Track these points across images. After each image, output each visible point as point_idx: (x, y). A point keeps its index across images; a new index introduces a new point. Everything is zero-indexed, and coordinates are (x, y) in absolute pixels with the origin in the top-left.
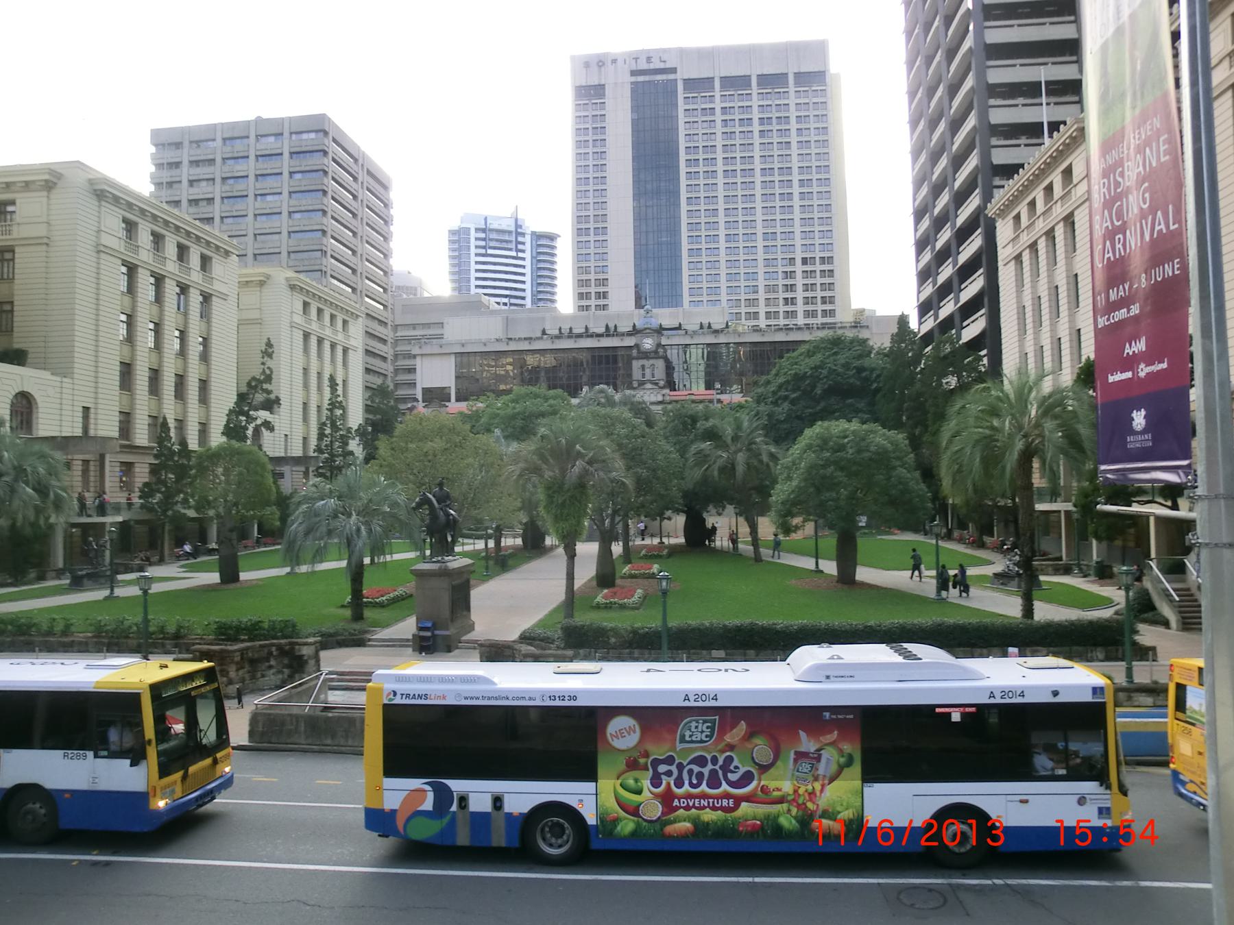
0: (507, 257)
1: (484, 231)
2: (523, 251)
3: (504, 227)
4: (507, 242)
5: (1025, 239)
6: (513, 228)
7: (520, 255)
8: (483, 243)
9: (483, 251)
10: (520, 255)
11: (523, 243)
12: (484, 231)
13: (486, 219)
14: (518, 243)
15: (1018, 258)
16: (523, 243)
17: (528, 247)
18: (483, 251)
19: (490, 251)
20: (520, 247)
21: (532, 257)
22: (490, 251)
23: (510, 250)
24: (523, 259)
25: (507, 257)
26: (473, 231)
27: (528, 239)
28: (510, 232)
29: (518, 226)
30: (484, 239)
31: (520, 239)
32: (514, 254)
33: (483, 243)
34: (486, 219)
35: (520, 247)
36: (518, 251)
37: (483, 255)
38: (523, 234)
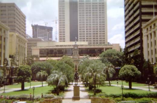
5: (149, 32)
15: (147, 36)
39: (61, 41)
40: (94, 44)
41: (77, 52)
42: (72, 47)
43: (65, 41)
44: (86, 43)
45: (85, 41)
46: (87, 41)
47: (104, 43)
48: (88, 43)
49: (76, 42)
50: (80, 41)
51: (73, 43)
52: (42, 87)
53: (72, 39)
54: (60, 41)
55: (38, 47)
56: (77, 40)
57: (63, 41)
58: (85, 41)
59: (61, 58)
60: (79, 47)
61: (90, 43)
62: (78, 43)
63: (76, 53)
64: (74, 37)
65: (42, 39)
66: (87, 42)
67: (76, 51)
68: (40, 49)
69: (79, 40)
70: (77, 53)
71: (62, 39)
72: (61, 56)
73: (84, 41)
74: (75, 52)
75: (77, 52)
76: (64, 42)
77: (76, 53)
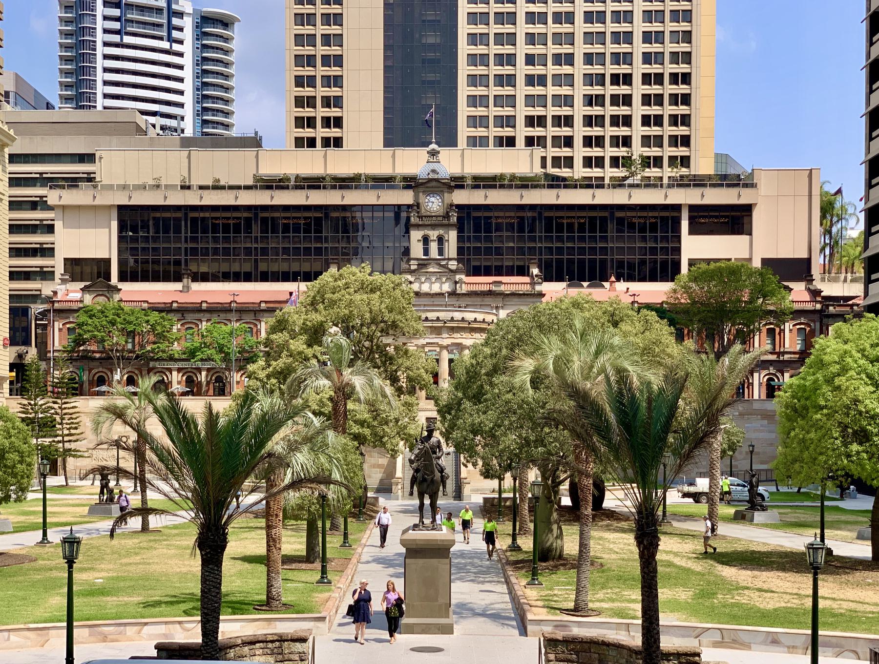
2: (181, 42)
4: (154, 25)
7: (176, 47)
8: (116, 25)
9: (116, 38)
10: (176, 47)
11: (181, 29)
14: (171, 27)
16: (181, 29)
17: (188, 35)
18: (116, 38)
19: (128, 39)
20: (175, 34)
22: (128, 39)
23: (161, 38)
24: (181, 55)
27: (187, 23)
28: (159, 10)
30: (118, 19)
31: (175, 21)
32: (165, 45)
33: (116, 25)
35: (175, 34)
36: (171, 40)
37: (117, 45)
38: (180, 15)
39: (312, 143)
40: (596, 172)
41: (440, 240)
42: (406, 197)
43: (338, 142)
44: (520, 162)
45: (520, 142)
46: (530, 141)
47: (685, 161)
48: (544, 159)
49: (434, 153)
50: (473, 142)
51: (412, 161)
52: (144, 537)
53: (400, 131)
54: (299, 142)
55: (110, 187)
56: (450, 140)
57: (326, 142)
58: (520, 142)
59: (301, 287)
60: (461, 197)
61: (557, 162)
62: (450, 162)
63: (434, 246)
64: (418, 105)
65: (141, 120)
66: (539, 152)
67: (434, 234)
68: (122, 209)
69: (464, 131)
70: (441, 251)
71: (317, 123)
72: (308, 277)
73: (511, 142)
74: (426, 240)
75: (440, 240)
76: (332, 151)
77: (434, 246)
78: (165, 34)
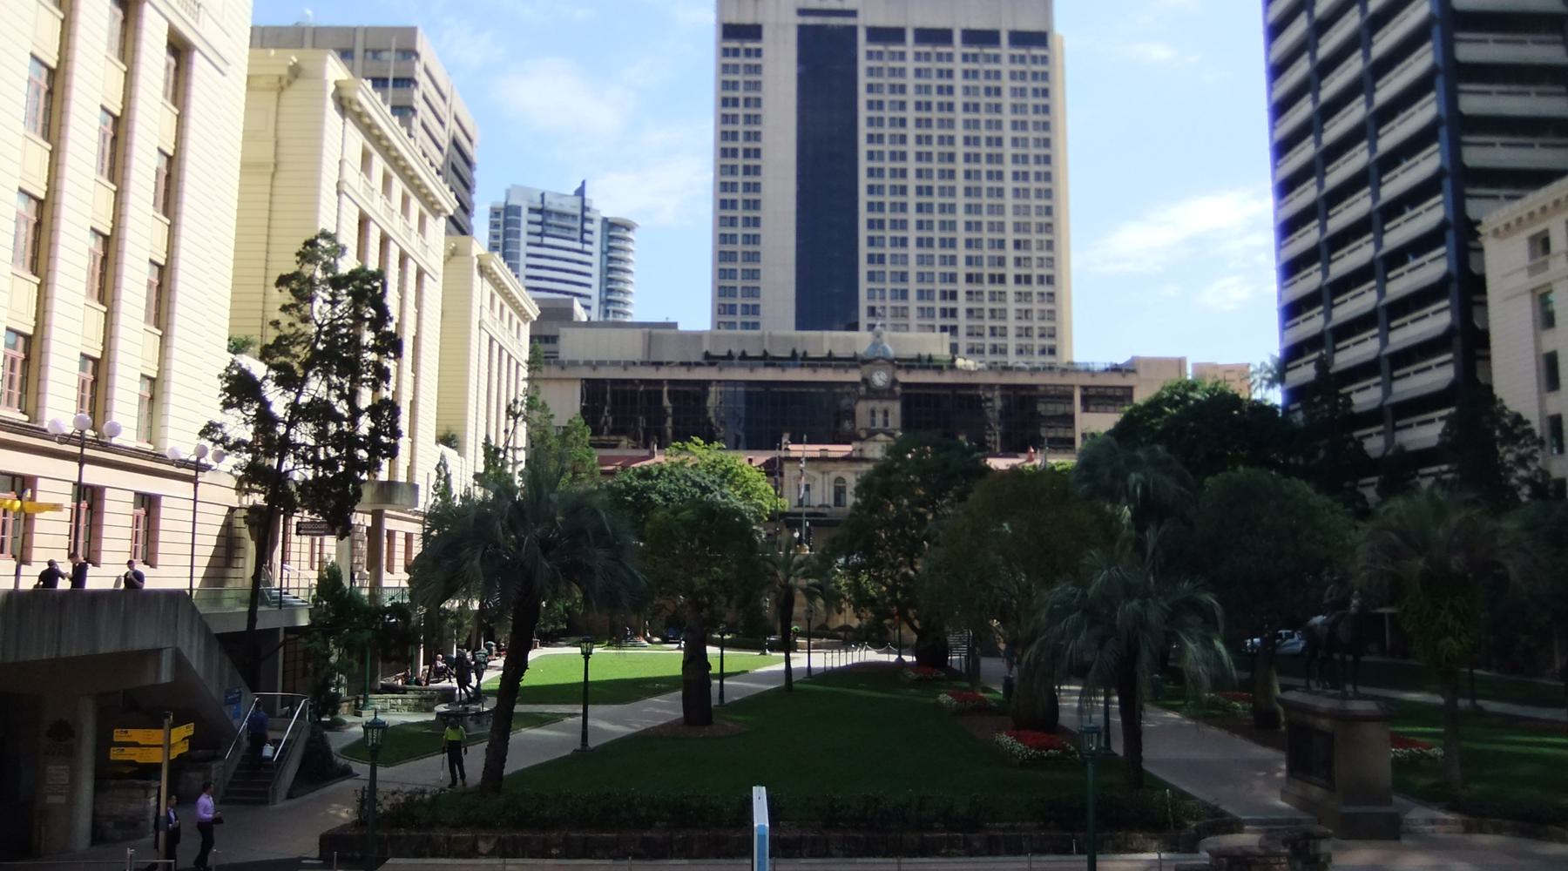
0: (568, 249)
1: (540, 211)
2: (590, 243)
3: (567, 209)
4: (569, 229)
6: (578, 212)
12: (540, 211)
13: (543, 195)
21: (602, 253)
25: (568, 249)
26: (524, 212)
28: (574, 217)
29: (584, 208)
32: (578, 245)
34: (543, 195)
36: (583, 241)
78: (577, 235)
